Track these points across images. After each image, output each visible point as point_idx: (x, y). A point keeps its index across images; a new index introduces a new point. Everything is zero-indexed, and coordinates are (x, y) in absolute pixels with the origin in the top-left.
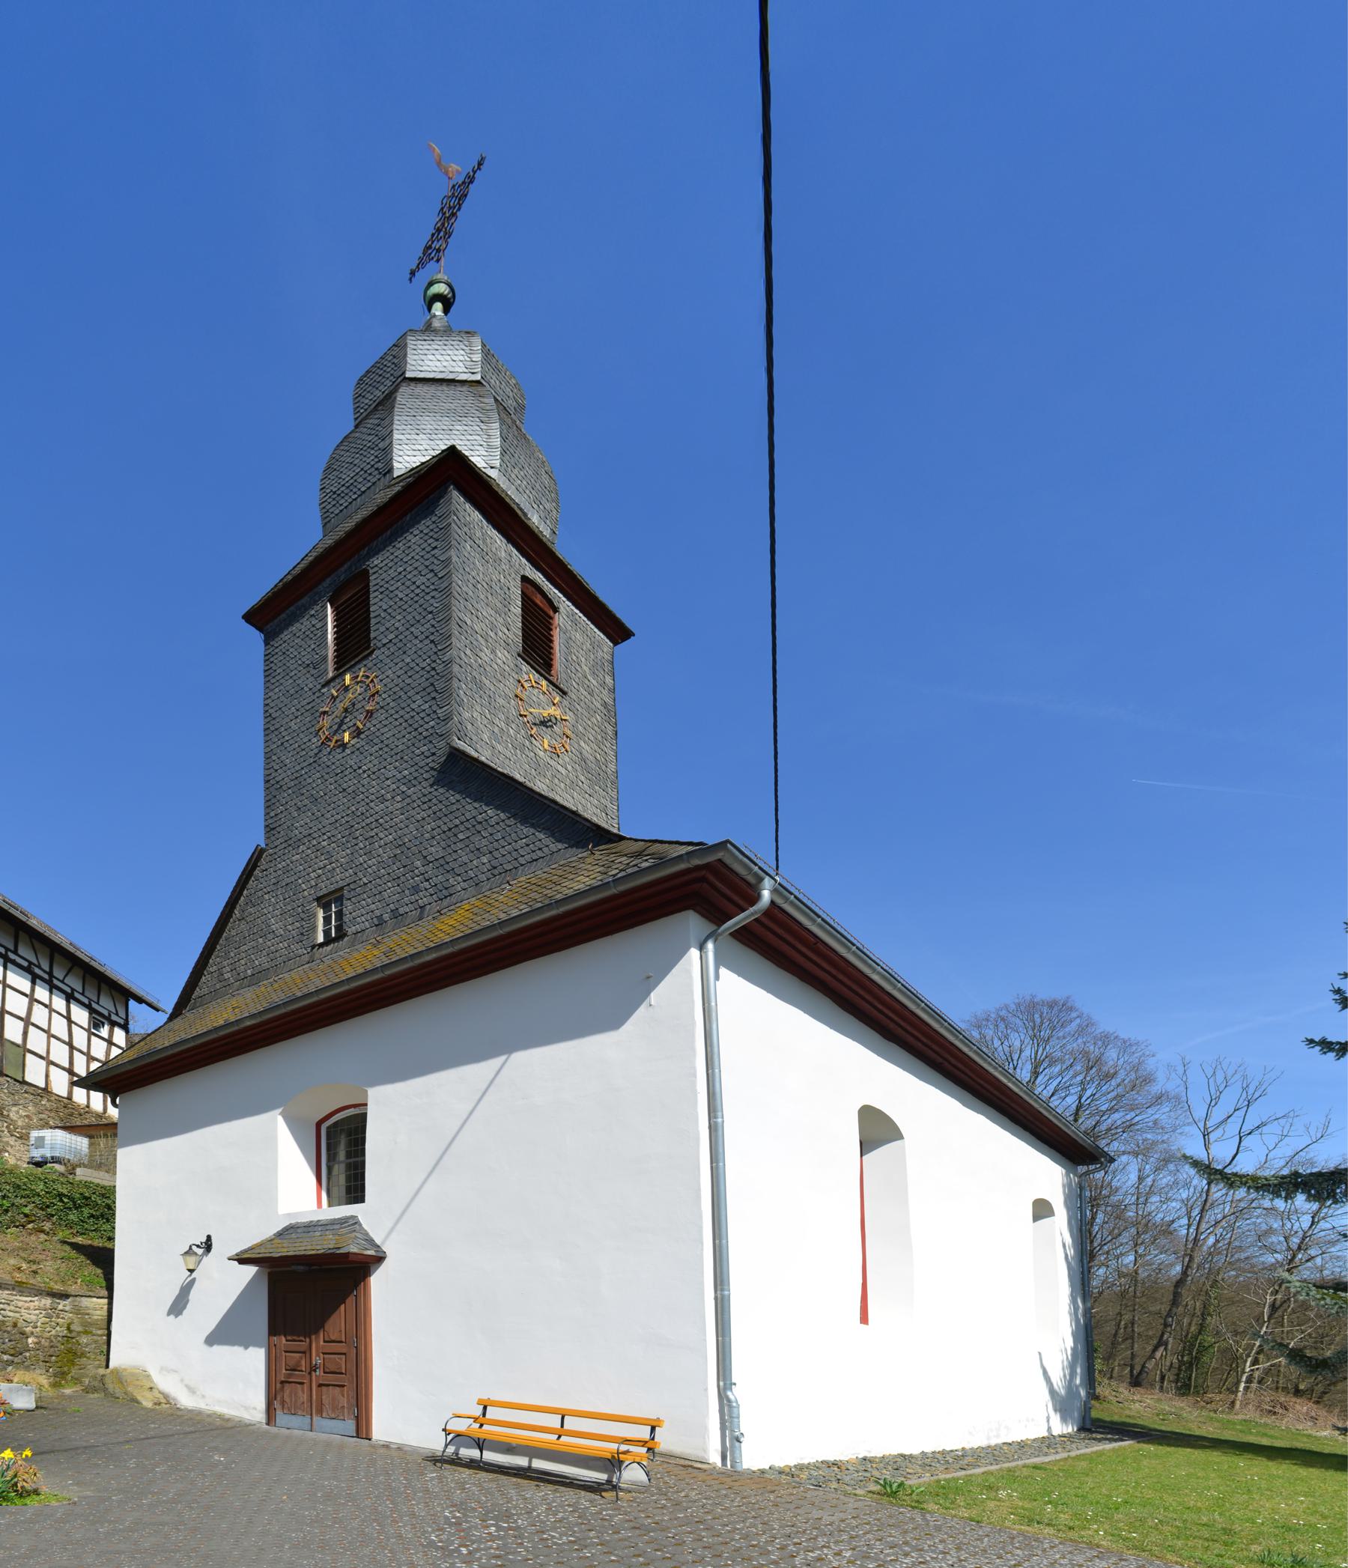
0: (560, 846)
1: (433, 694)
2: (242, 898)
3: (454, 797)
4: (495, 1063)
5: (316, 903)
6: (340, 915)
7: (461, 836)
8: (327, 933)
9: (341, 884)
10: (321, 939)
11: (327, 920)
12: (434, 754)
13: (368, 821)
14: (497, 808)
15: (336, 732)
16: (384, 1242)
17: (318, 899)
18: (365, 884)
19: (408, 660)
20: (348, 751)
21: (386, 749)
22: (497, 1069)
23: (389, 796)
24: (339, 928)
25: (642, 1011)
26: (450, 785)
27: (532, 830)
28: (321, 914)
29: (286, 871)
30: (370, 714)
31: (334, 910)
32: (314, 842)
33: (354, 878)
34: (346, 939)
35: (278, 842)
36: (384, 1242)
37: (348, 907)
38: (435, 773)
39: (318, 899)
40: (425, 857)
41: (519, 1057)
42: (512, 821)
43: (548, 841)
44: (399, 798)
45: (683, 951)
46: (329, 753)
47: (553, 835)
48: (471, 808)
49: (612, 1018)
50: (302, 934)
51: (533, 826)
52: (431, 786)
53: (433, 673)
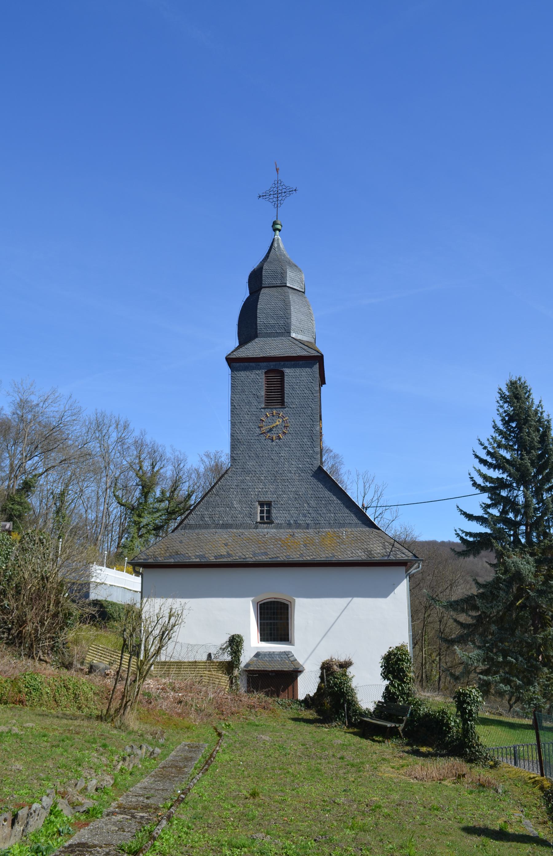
0: (359, 522)
1: (312, 441)
2: (217, 485)
3: (321, 486)
4: (347, 600)
5: (257, 503)
6: (269, 512)
7: (323, 502)
8: (262, 518)
9: (271, 499)
10: (259, 520)
11: (262, 512)
12: (312, 464)
13: (284, 478)
14: (337, 498)
15: (268, 432)
16: (304, 664)
17: (259, 501)
18: (282, 504)
19: (301, 420)
20: (274, 443)
21: (292, 452)
22: (348, 603)
23: (293, 472)
24: (268, 518)
25: (392, 594)
26: (319, 480)
27: (349, 512)
28: (259, 509)
29: (243, 481)
30: (284, 433)
31: (265, 508)
32: (257, 475)
33: (277, 499)
34: (273, 525)
35: (238, 467)
36: (304, 664)
37: (274, 511)
38: (313, 473)
39: (259, 501)
40: (308, 504)
41: (356, 600)
42: (342, 505)
43: (355, 518)
44: (297, 475)
45: (404, 579)
46: (265, 439)
47: (356, 516)
48: (328, 493)
49: (385, 595)
50: (251, 514)
51: (350, 510)
52: (311, 477)
53: (311, 431)
